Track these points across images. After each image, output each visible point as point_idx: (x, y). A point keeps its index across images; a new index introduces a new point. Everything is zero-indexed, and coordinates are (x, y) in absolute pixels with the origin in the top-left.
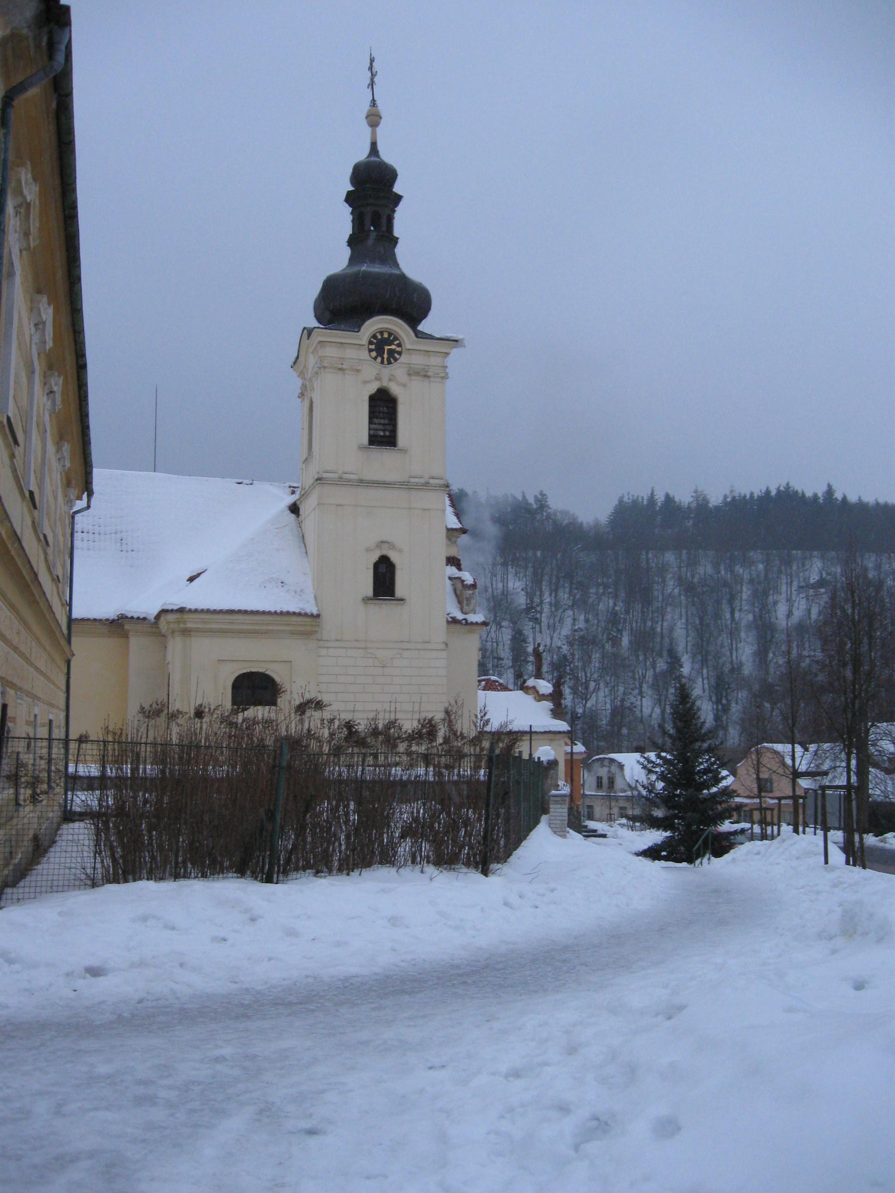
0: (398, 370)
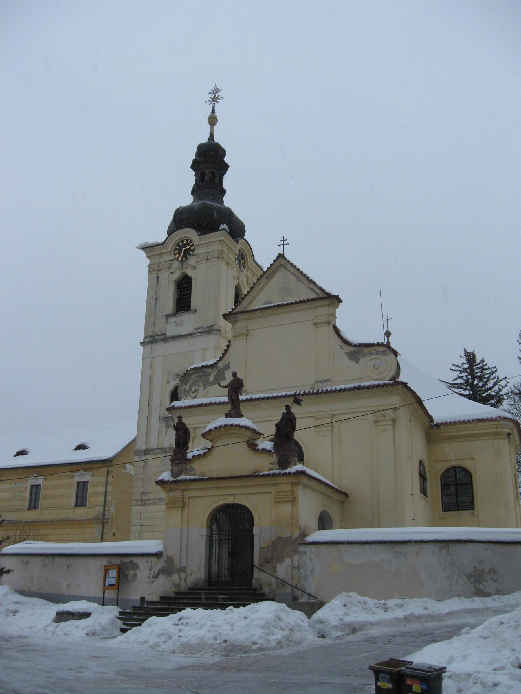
0: (192, 261)
